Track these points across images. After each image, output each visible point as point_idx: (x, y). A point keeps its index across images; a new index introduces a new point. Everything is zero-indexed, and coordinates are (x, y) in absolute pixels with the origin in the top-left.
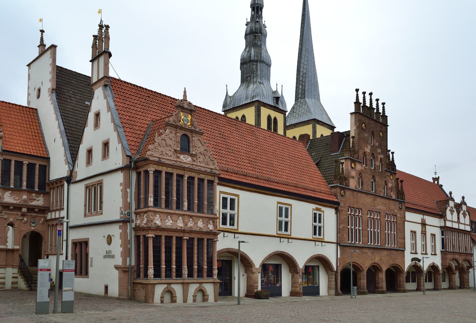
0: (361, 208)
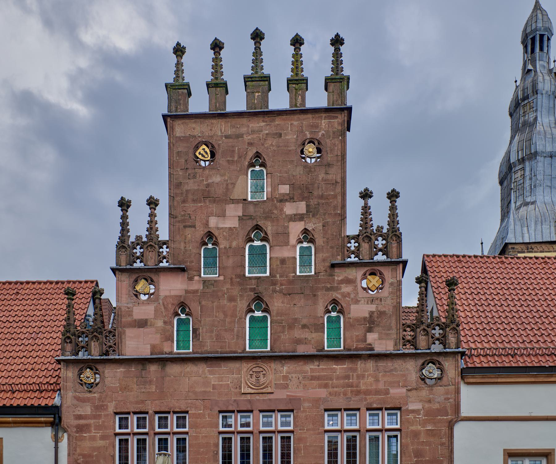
0: (183, 408)
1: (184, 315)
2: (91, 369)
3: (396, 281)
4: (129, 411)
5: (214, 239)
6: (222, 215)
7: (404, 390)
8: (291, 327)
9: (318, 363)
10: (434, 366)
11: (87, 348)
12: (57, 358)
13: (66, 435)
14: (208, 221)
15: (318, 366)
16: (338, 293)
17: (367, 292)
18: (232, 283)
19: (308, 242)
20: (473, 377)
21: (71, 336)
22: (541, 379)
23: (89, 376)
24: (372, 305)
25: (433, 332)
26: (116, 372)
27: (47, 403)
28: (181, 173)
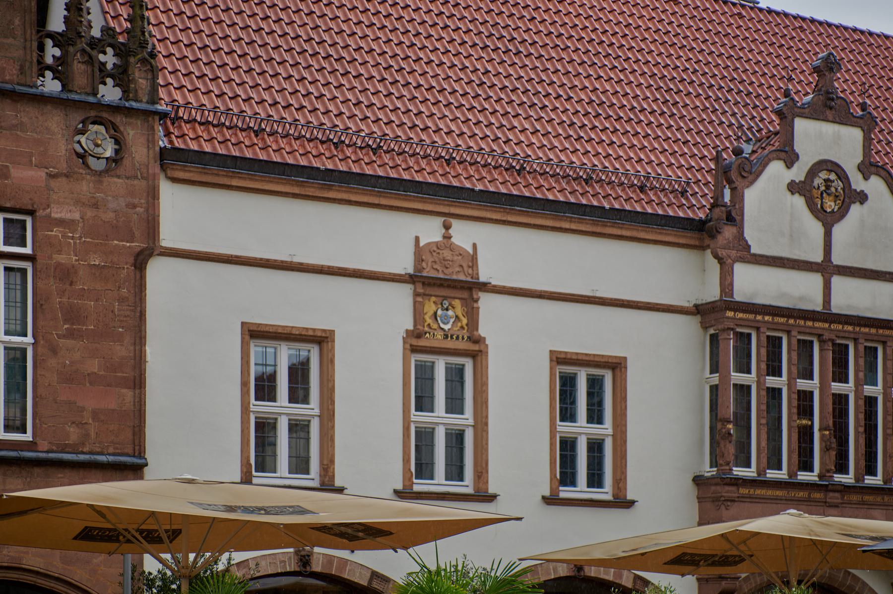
7: (42, 174)
22: (310, 192)
25: (102, 57)
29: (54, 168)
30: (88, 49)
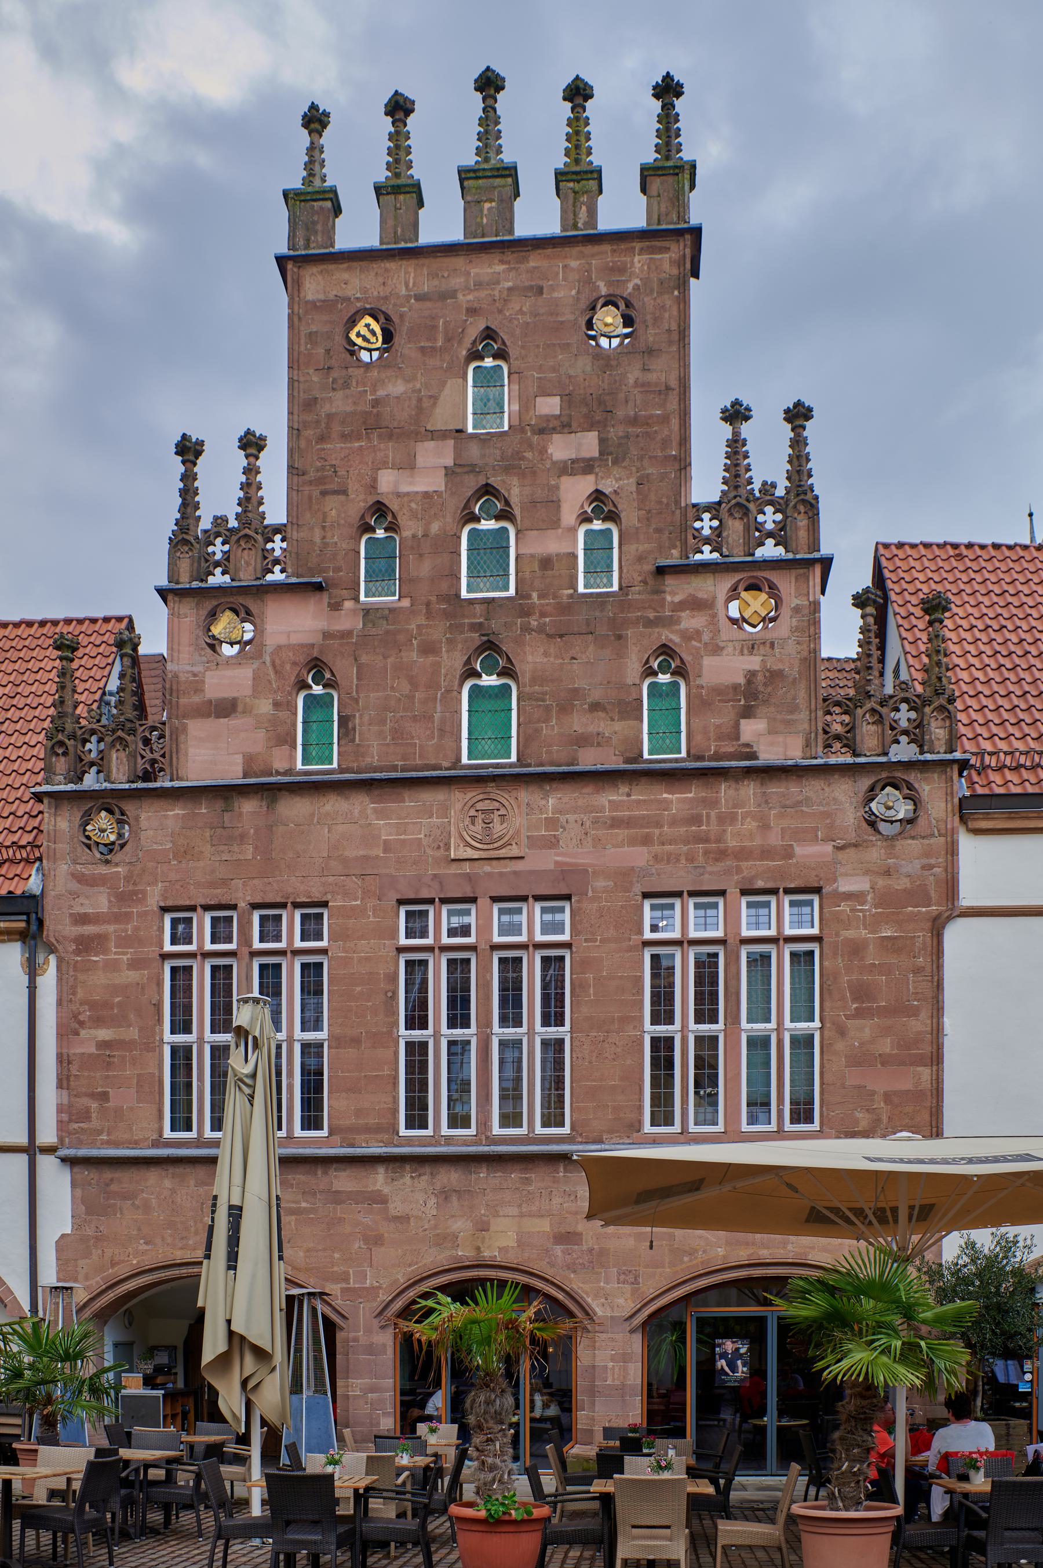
0: (317, 897)
1: (321, 687)
2: (110, 812)
3: (807, 603)
4: (193, 903)
5: (389, 519)
6: (409, 465)
7: (829, 848)
8: (565, 709)
9: (627, 790)
10: (897, 793)
11: (101, 764)
12: (38, 789)
13: (52, 959)
14: (375, 480)
15: (629, 795)
16: (672, 632)
17: (740, 628)
18: (429, 615)
19: (604, 520)
20: (987, 817)
21: (67, 741)
23: (104, 827)
24: (753, 658)
26: (166, 817)
27: (11, 889)
28: (315, 379)
29: (841, 839)
30: (878, 708)
